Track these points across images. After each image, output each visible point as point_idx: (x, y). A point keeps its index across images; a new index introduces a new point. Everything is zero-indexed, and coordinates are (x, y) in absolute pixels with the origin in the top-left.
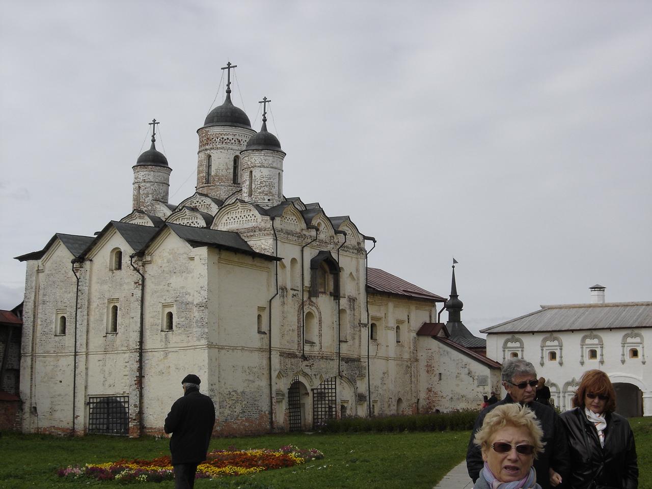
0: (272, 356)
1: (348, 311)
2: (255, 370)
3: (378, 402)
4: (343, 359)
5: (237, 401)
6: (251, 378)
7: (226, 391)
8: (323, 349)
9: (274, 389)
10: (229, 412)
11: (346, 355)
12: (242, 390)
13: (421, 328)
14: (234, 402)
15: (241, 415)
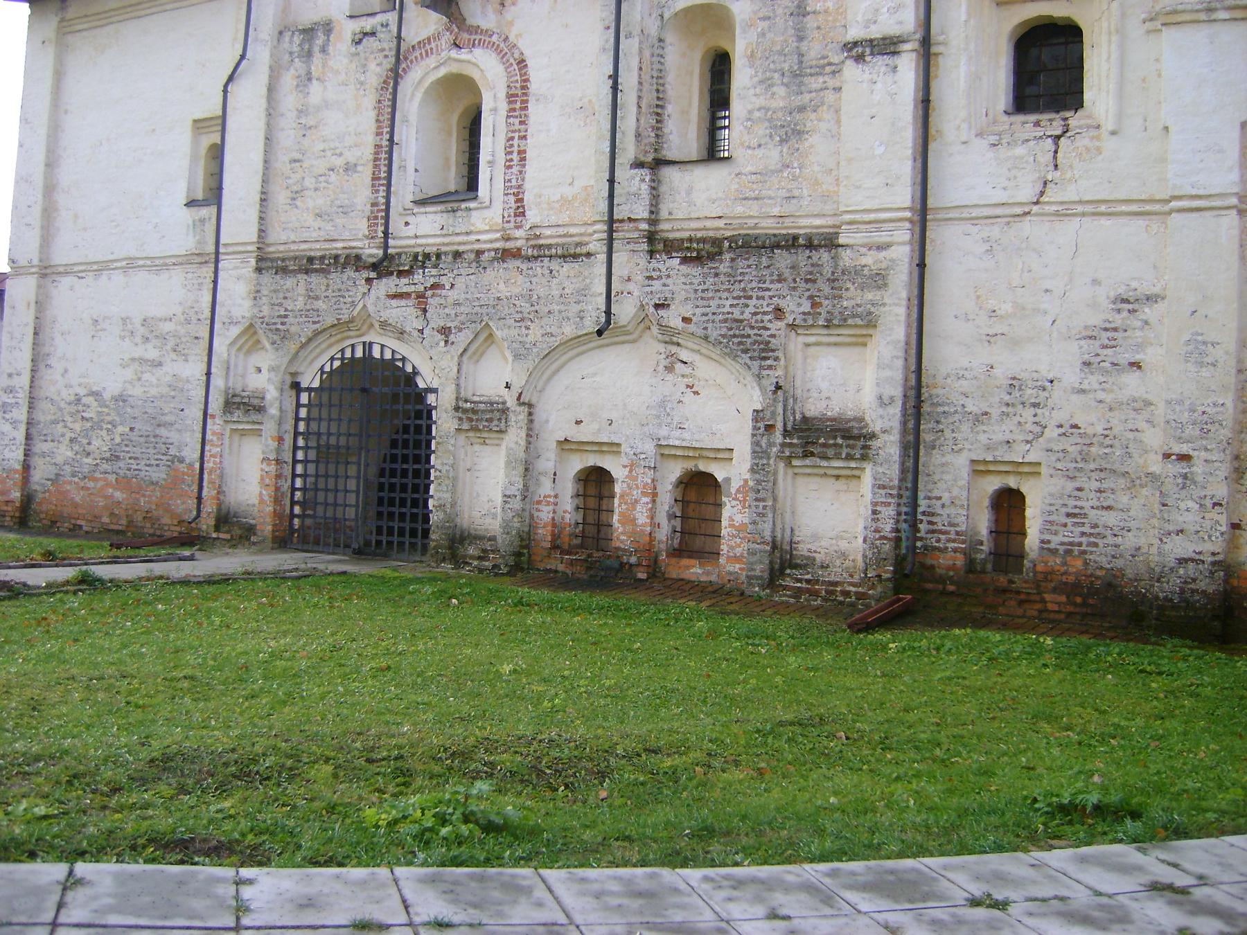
0: (221, 274)
2: (167, 327)
3: (1044, 470)
4: (670, 247)
5: (97, 426)
6: (152, 353)
7: (67, 395)
8: (533, 216)
9: (218, 382)
10: (70, 454)
11: (721, 223)
12: (116, 393)
14: (89, 424)
15: (105, 466)
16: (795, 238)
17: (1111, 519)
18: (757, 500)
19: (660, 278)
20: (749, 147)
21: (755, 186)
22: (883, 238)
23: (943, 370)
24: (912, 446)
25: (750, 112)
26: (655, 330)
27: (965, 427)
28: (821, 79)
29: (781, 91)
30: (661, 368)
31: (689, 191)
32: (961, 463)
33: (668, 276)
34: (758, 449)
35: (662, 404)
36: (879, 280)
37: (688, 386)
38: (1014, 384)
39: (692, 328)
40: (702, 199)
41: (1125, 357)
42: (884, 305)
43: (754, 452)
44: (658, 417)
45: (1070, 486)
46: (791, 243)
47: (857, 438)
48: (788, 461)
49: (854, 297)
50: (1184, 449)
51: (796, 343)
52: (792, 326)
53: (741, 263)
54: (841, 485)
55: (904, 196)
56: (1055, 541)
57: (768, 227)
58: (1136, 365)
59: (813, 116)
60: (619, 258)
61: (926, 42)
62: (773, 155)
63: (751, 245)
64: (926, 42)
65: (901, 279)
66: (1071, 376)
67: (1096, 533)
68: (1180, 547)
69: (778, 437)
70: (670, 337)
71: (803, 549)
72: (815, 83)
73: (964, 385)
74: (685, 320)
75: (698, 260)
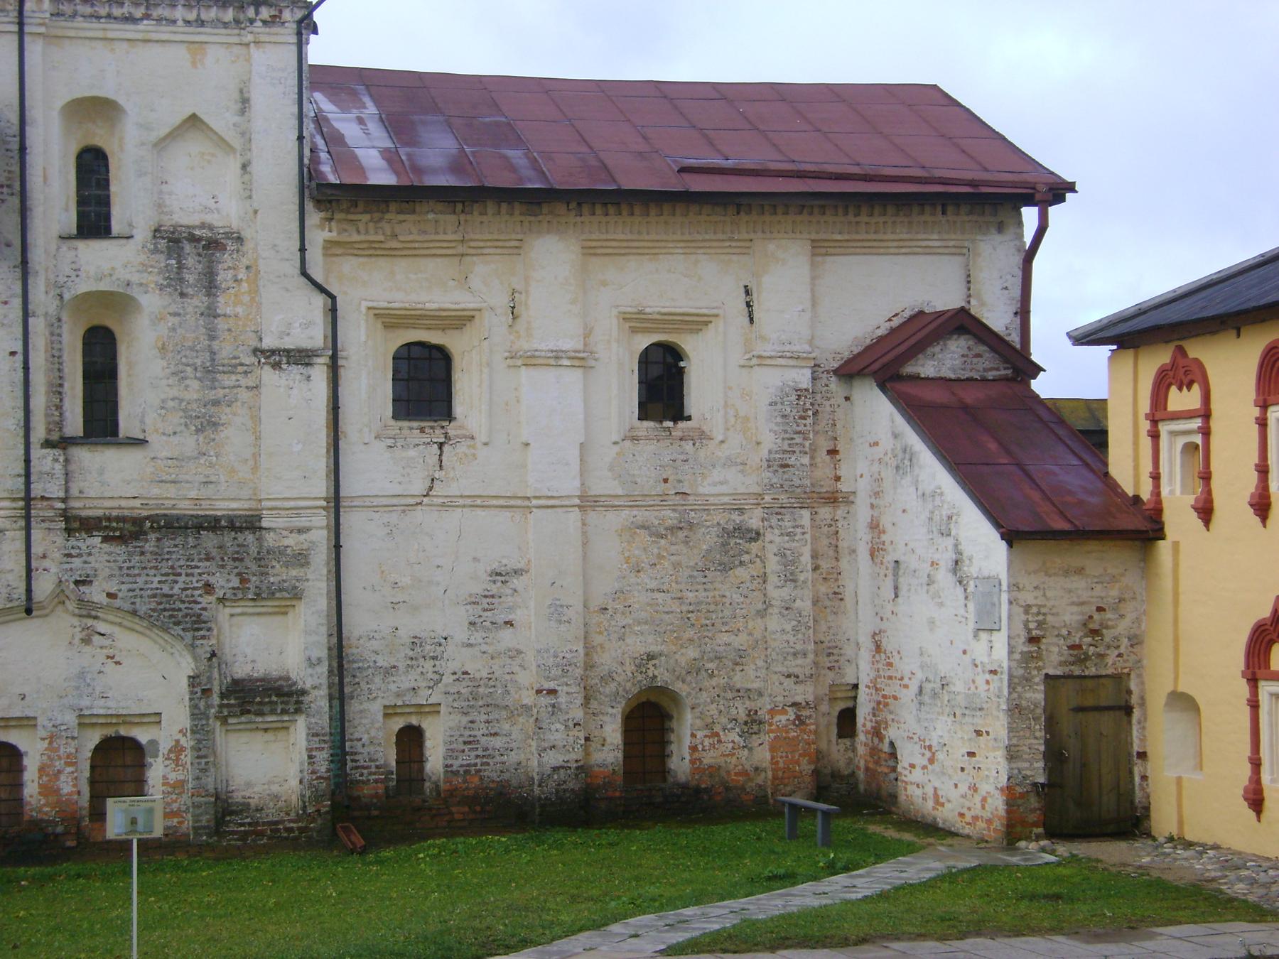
1: (151, 302)
3: (443, 709)
4: (88, 525)
11: (137, 503)
13: (881, 339)
16: (217, 519)
17: (498, 742)
18: (198, 757)
19: (79, 555)
20: (164, 434)
21: (171, 470)
22: (302, 522)
23: (356, 634)
24: (340, 697)
25: (163, 401)
26: (71, 606)
27: (378, 679)
28: (234, 377)
29: (195, 384)
30: (77, 641)
31: (101, 472)
32: (376, 708)
33: (90, 554)
34: (196, 711)
35: (82, 675)
36: (301, 558)
37: (108, 657)
38: (416, 642)
39: (118, 603)
40: (110, 479)
41: (501, 618)
42: (308, 580)
43: (193, 715)
44: (77, 688)
45: (465, 720)
46: (213, 524)
47: (290, 694)
48: (224, 721)
49: (280, 573)
50: (552, 685)
51: (224, 613)
52: (221, 600)
53: (167, 543)
54: (269, 736)
55: (320, 487)
56: (456, 764)
57: (185, 508)
58: (509, 623)
59: (228, 410)
60: (36, 534)
61: (334, 357)
62: (188, 443)
63: (171, 526)
64: (334, 357)
65: (321, 557)
66: (460, 633)
67: (487, 754)
68: (554, 759)
69: (216, 700)
70: (88, 610)
71: (238, 797)
72: (229, 380)
73: (375, 644)
74: (110, 595)
75: (122, 539)
